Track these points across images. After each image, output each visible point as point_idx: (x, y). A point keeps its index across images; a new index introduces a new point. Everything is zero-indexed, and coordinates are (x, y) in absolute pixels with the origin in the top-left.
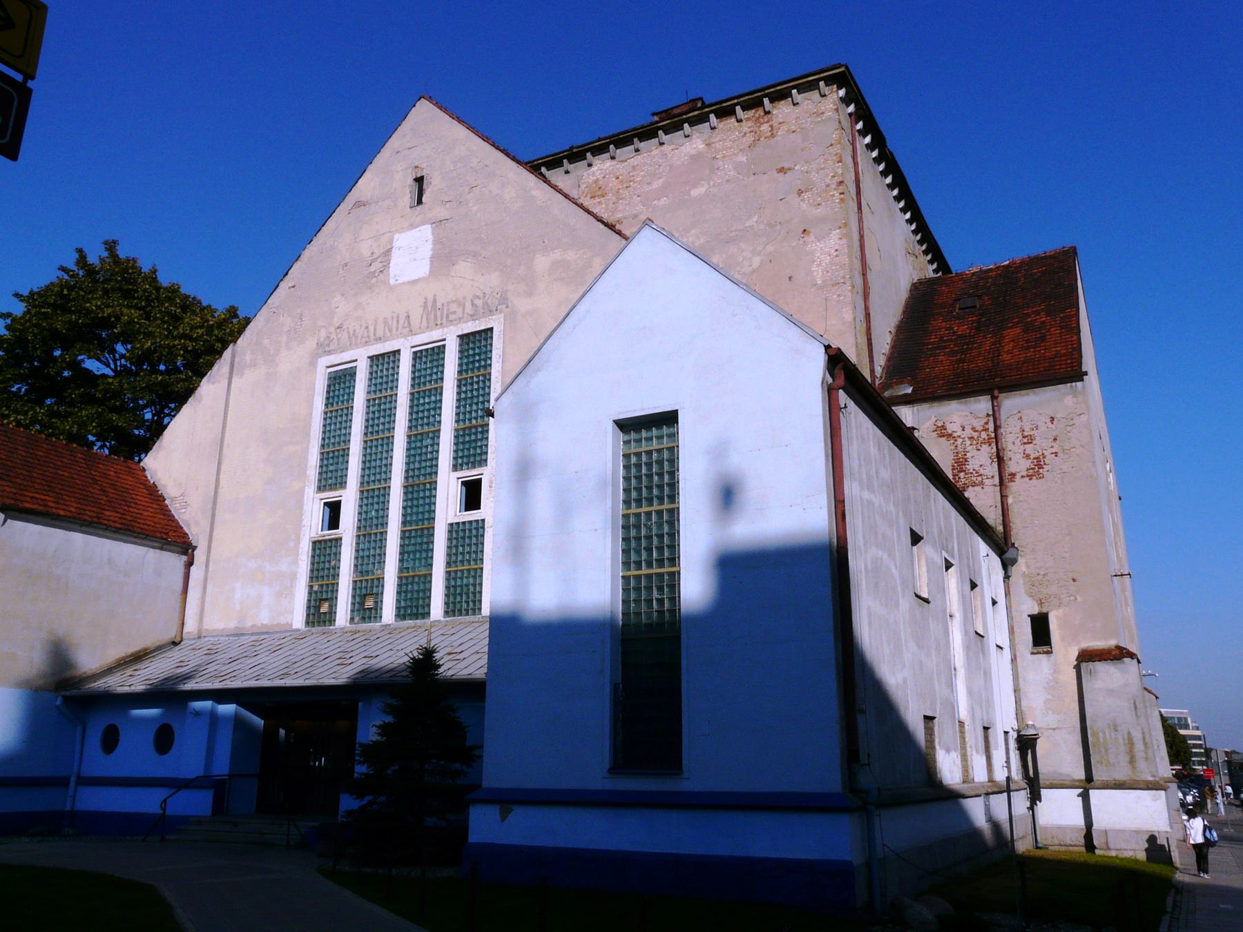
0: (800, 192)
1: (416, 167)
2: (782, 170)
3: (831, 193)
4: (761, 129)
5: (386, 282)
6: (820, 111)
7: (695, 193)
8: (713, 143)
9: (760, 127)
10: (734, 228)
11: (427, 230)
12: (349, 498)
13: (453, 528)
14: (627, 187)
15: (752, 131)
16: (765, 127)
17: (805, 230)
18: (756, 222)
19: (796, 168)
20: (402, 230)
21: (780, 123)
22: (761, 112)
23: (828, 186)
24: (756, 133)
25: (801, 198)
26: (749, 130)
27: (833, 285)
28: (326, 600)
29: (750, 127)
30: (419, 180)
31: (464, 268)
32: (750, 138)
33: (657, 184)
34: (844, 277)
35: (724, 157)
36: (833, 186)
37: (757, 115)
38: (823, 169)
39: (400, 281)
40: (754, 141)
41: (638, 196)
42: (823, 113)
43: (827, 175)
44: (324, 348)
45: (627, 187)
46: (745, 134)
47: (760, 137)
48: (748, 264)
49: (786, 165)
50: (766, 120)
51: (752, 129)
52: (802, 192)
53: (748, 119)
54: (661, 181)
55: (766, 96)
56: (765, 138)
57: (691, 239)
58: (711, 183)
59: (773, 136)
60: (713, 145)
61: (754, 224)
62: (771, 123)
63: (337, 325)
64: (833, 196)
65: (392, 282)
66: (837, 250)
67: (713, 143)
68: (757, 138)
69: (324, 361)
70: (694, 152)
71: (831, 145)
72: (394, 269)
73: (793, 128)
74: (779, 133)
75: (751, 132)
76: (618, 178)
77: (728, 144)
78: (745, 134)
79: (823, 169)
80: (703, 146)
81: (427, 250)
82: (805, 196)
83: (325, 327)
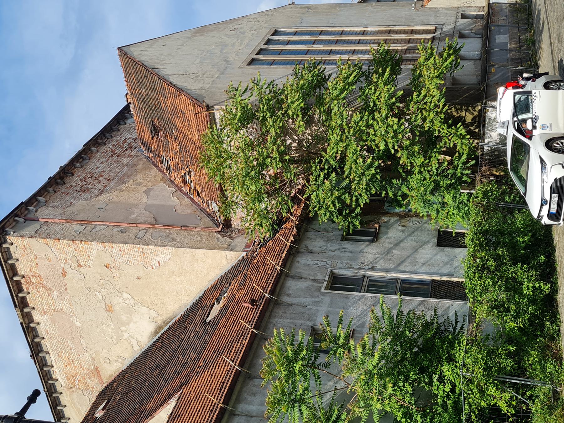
0: (80, 266)
2: (64, 274)
4: (35, 282)
6: (23, 247)
8: (44, 310)
14: (73, 361)
15: (36, 288)
16: (33, 280)
17: (106, 266)
19: (62, 265)
22: (23, 281)
23: (76, 250)
25: (83, 265)
29: (33, 288)
32: (42, 290)
34: (139, 248)
36: (76, 246)
37: (25, 283)
40: (42, 287)
41: (79, 356)
42: (24, 246)
45: (73, 361)
46: (37, 291)
47: (40, 283)
48: (128, 300)
49: (60, 271)
50: (28, 279)
51: (34, 287)
52: (80, 264)
53: (27, 288)
55: (11, 278)
57: (110, 330)
58: (72, 314)
59: (40, 276)
60: (45, 310)
62: (31, 276)
64: (82, 247)
66: (120, 250)
67: (44, 310)
68: (41, 285)
73: (34, 264)
74: (38, 272)
75: (36, 288)
76: (66, 366)
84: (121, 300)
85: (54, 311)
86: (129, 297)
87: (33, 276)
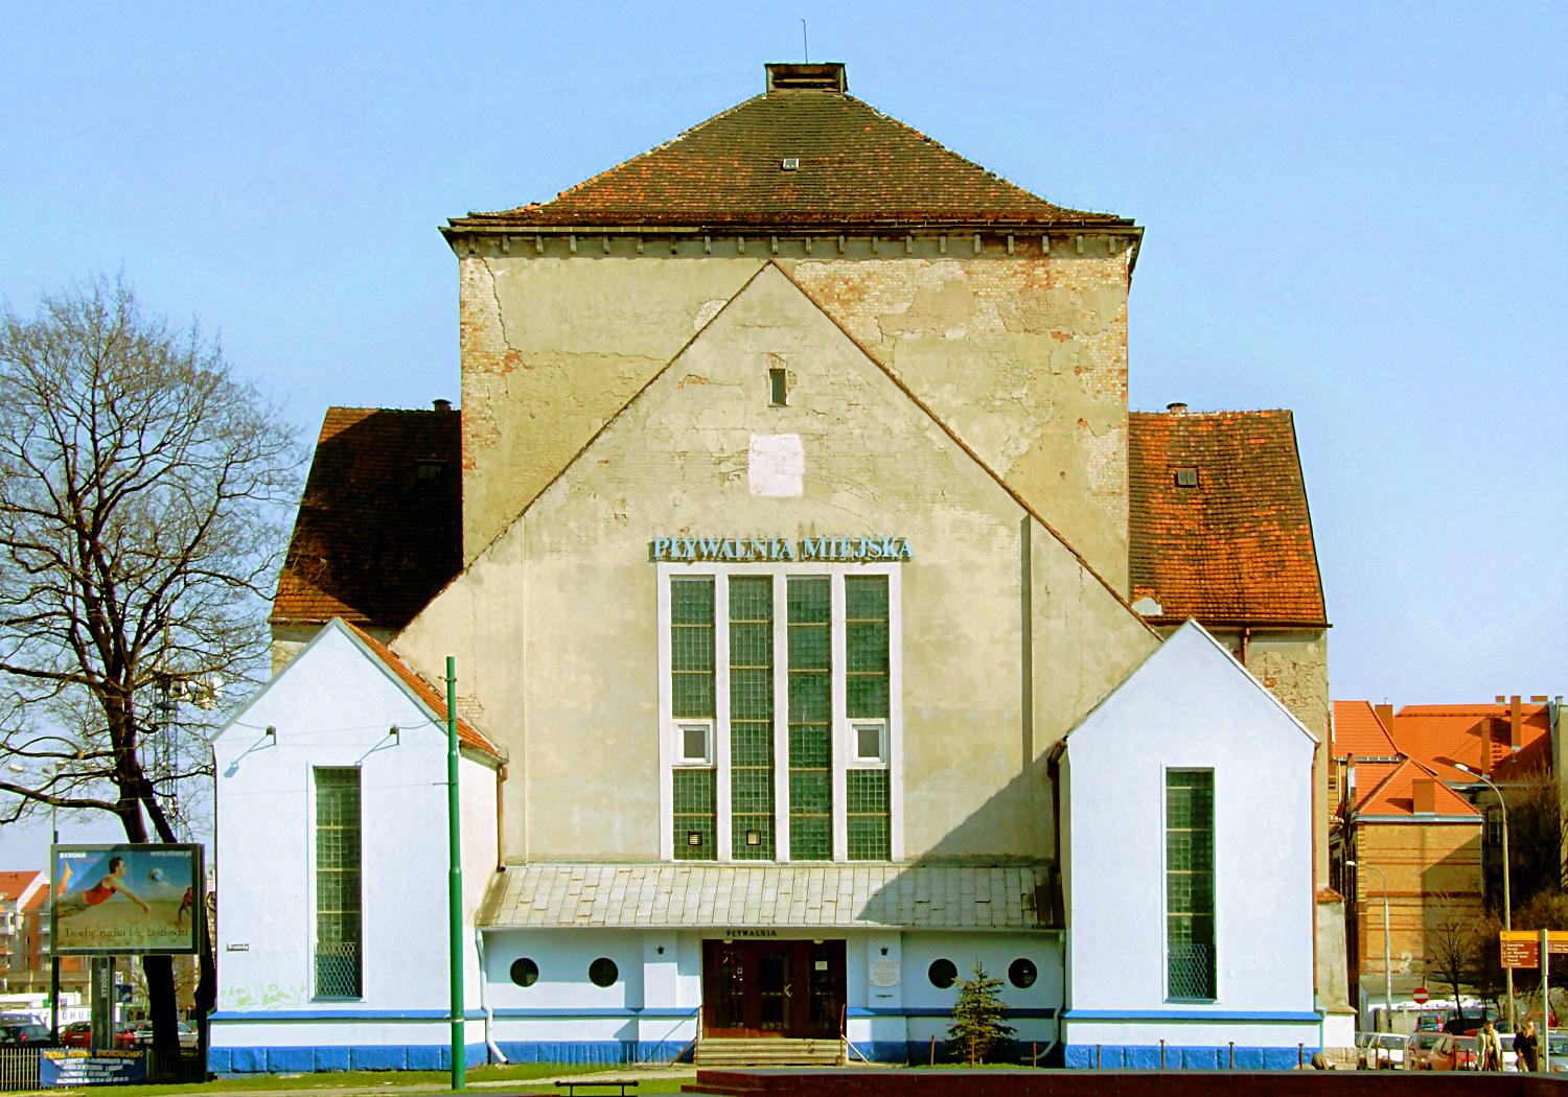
0: (1078, 370)
1: (773, 355)
3: (1113, 382)
5: (744, 490)
7: (950, 335)
9: (1033, 270)
10: (999, 395)
11: (795, 441)
12: (721, 732)
13: (854, 776)
15: (1023, 272)
16: (1040, 271)
17: (1081, 420)
18: (1026, 394)
20: (761, 432)
21: (1058, 272)
23: (1110, 371)
24: (1028, 275)
26: (1020, 269)
27: (1108, 494)
28: (695, 833)
30: (778, 376)
31: (845, 498)
32: (1021, 281)
33: (902, 307)
34: (1121, 487)
35: (986, 296)
38: (1103, 348)
39: (764, 494)
43: (1109, 357)
44: (658, 552)
46: (1016, 272)
49: (1065, 331)
51: (1024, 269)
54: (906, 305)
56: (1040, 286)
61: (1023, 396)
63: (681, 526)
64: (1115, 385)
65: (753, 492)
67: (974, 272)
69: (666, 571)
70: (949, 278)
71: (1117, 320)
72: (754, 477)
74: (1056, 285)
75: (1023, 272)
77: (996, 281)
78: (1016, 272)
79: (1103, 348)
80: (962, 272)
81: (798, 465)
82: (1085, 376)
83: (662, 525)
84: (1014, 432)
85: (975, 294)
86: (1024, 449)
87: (1047, 272)
